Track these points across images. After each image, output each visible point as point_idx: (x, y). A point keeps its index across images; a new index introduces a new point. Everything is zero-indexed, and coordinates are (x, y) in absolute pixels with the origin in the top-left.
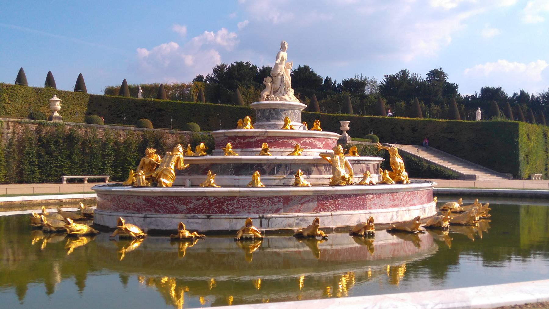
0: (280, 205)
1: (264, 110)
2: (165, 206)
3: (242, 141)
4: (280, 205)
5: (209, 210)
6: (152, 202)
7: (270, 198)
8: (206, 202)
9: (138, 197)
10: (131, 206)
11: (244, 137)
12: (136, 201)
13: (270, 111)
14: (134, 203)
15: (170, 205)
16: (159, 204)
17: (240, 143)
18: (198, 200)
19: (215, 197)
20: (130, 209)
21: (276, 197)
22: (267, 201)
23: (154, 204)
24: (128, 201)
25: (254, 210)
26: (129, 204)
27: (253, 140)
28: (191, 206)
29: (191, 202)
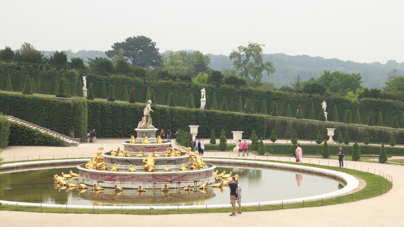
0: (198, 177)
1: (147, 133)
2: (162, 179)
3: (153, 149)
4: (198, 177)
5: (179, 180)
6: (157, 178)
7: (196, 174)
8: (178, 177)
9: (150, 176)
10: (146, 180)
11: (154, 147)
12: (149, 178)
13: (150, 133)
14: (147, 178)
15: (164, 179)
16: (160, 178)
17: (152, 150)
18: (175, 176)
19: (181, 175)
20: (145, 181)
21: (197, 173)
22: (195, 175)
23: (158, 179)
24: (144, 178)
25: (192, 179)
26: (144, 179)
27: (157, 148)
28: (173, 178)
29: (173, 177)
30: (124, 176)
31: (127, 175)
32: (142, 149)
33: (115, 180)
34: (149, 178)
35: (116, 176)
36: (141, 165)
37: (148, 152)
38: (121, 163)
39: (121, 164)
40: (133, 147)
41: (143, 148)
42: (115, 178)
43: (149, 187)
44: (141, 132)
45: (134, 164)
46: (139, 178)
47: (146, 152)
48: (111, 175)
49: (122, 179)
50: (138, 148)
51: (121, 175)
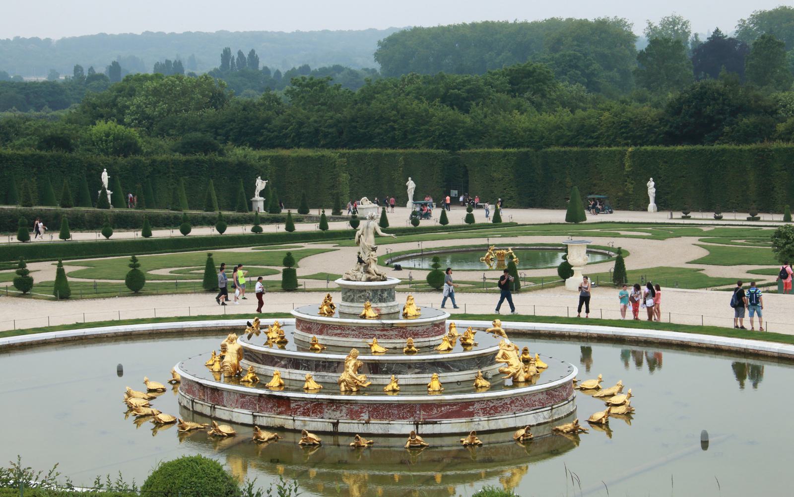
2: (558, 395)
9: (542, 393)
10: (537, 403)
12: (541, 397)
24: (534, 399)
26: (535, 401)
30: (495, 402)
31: (501, 399)
32: (427, 329)
33: (471, 414)
34: (541, 397)
35: (473, 405)
36: (470, 369)
37: (436, 336)
38: (417, 370)
39: (418, 373)
40: (402, 328)
41: (428, 327)
42: (471, 409)
43: (545, 418)
44: (377, 290)
45: (456, 369)
46: (525, 401)
47: (433, 336)
48: (458, 403)
49: (491, 409)
50: (417, 329)
51: (488, 400)
